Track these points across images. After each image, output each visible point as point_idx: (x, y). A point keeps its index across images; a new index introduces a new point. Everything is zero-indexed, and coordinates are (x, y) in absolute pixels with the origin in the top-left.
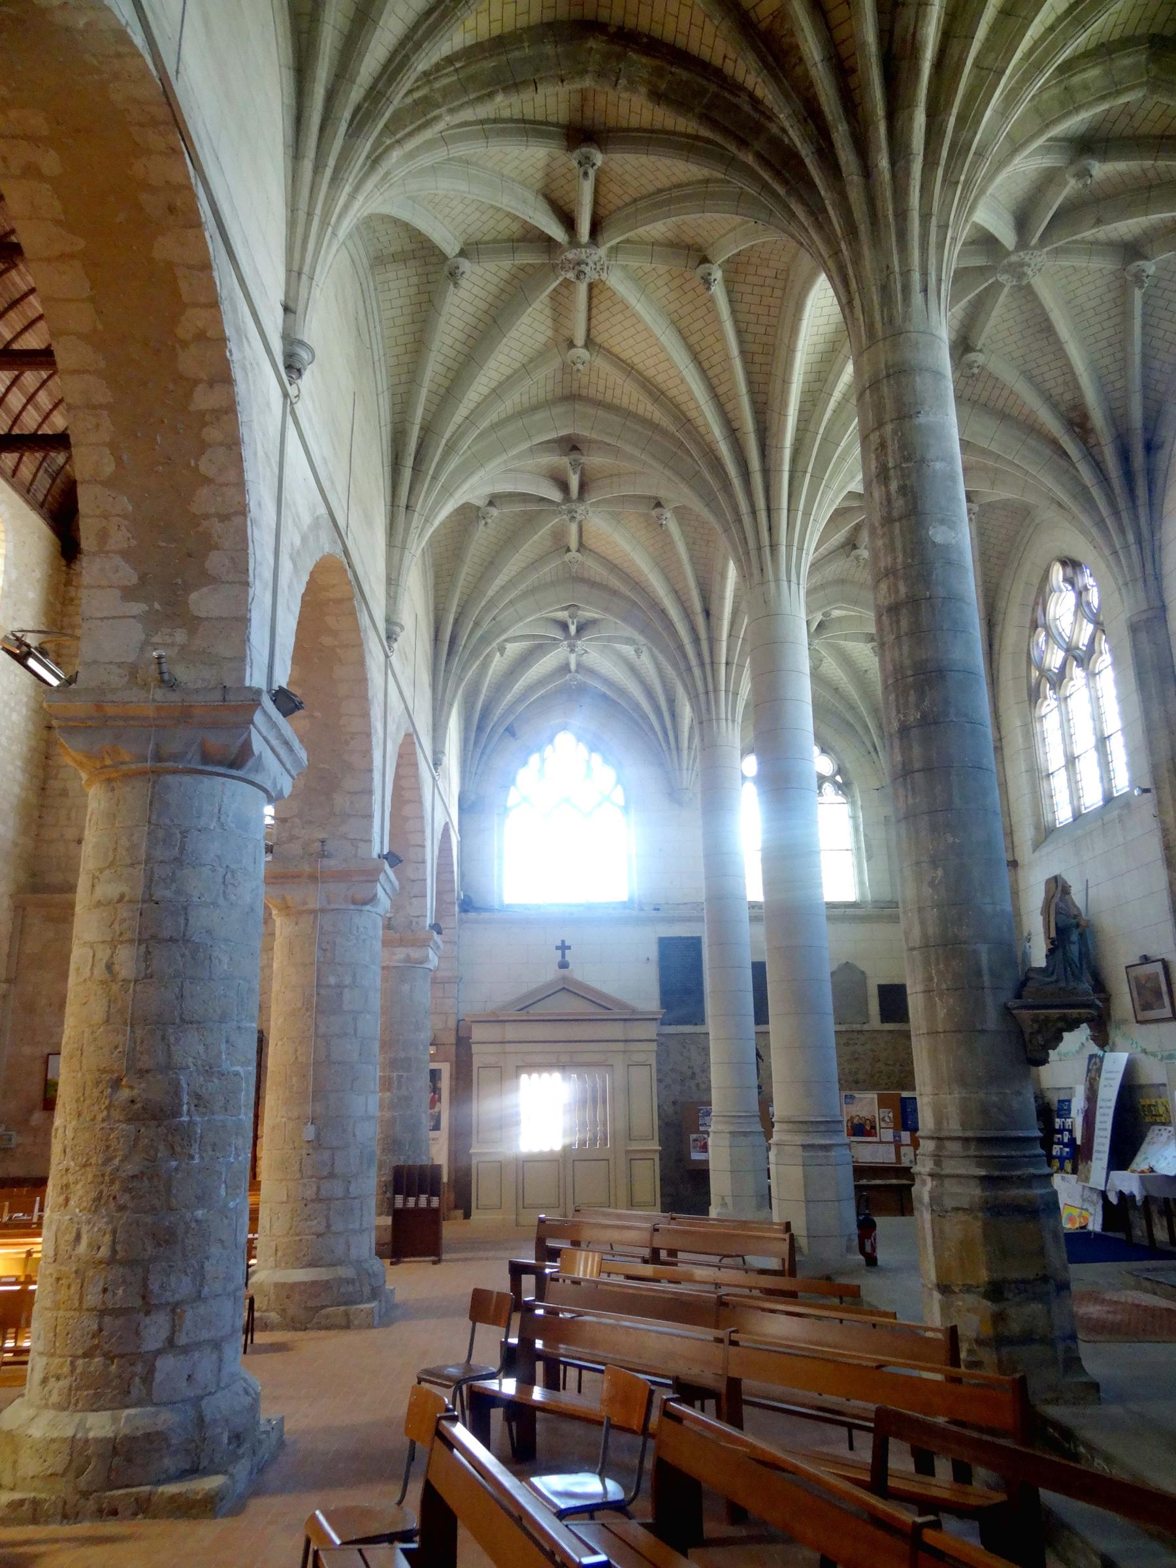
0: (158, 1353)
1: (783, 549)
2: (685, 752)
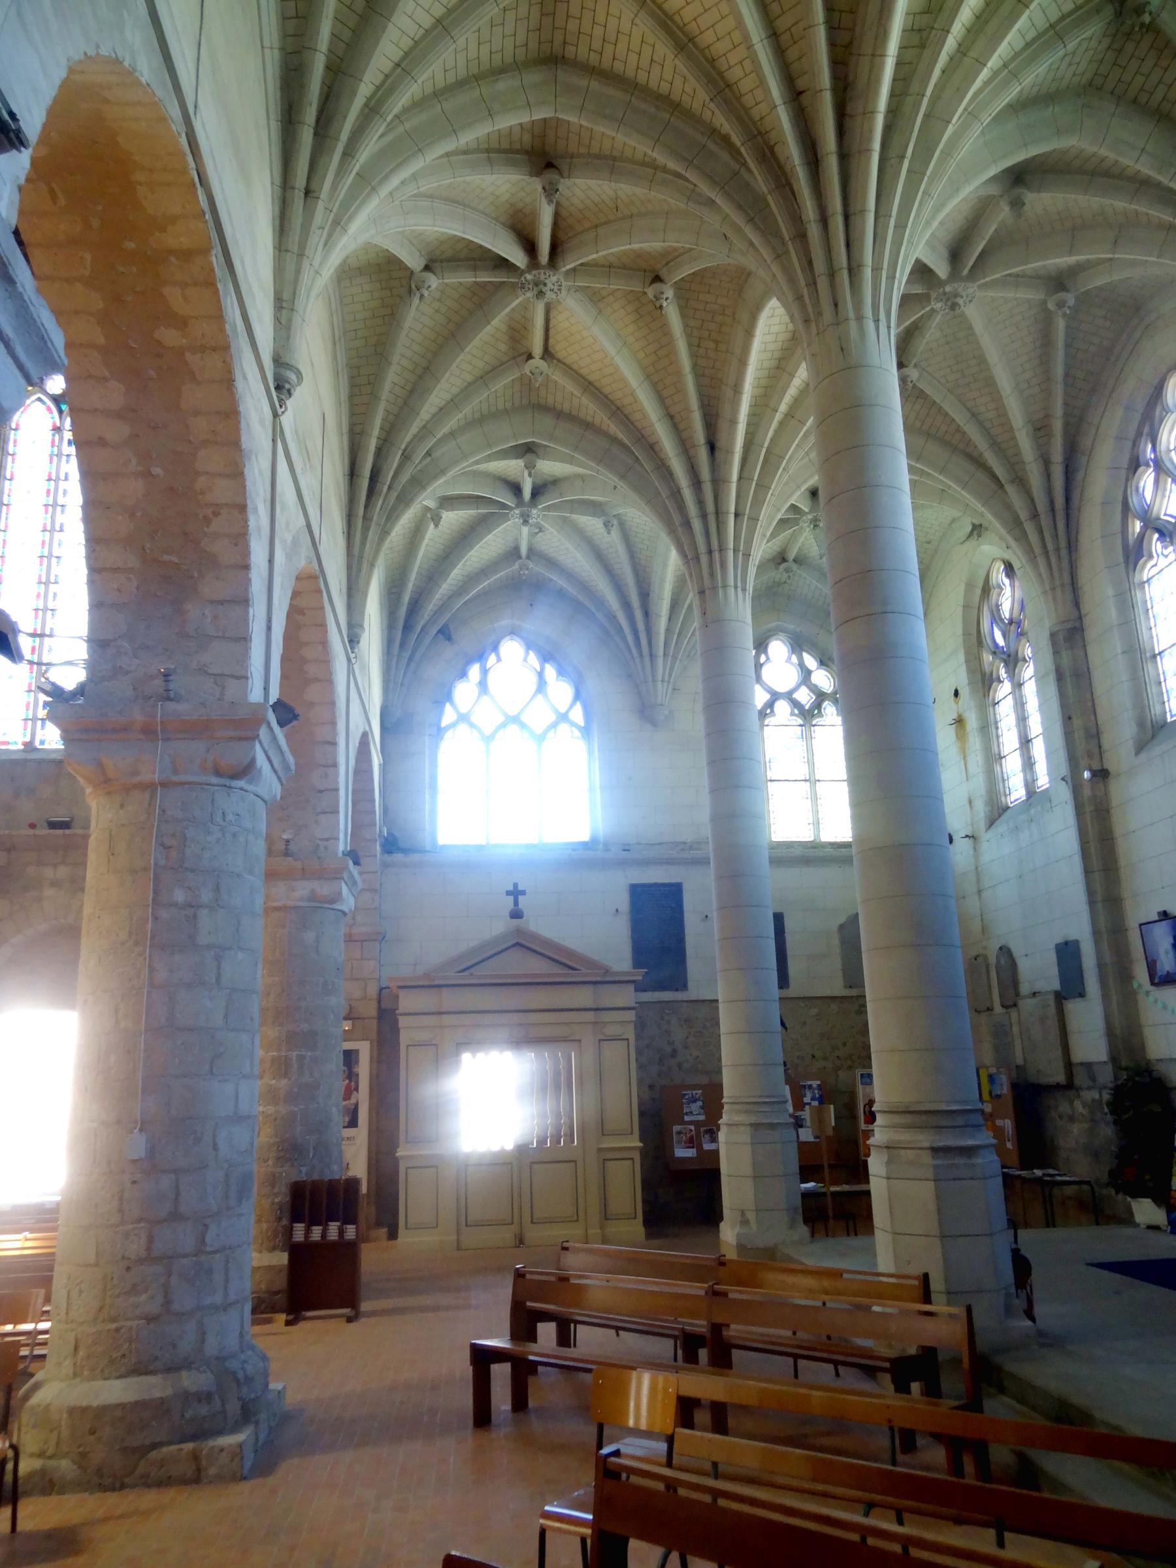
1: (868, 272)
2: (660, 661)
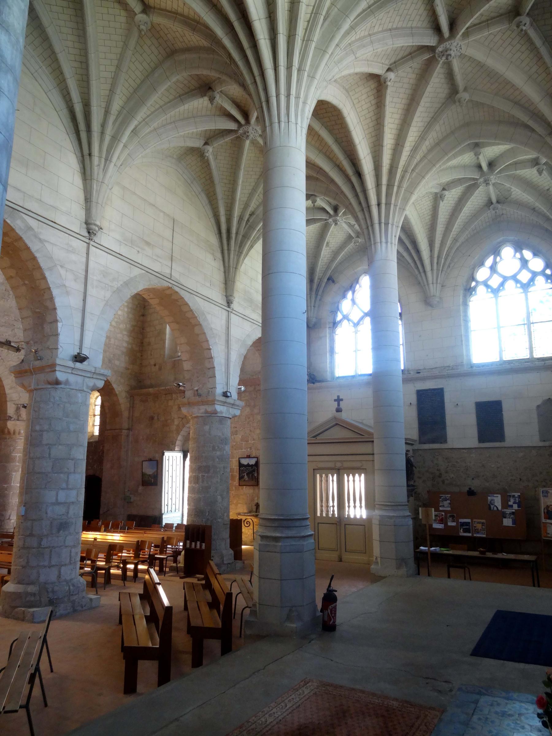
1: (273, 100)
2: (429, 274)
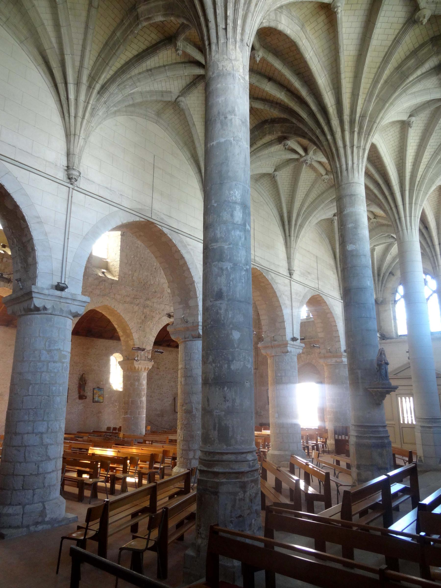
0: (192, 459)
